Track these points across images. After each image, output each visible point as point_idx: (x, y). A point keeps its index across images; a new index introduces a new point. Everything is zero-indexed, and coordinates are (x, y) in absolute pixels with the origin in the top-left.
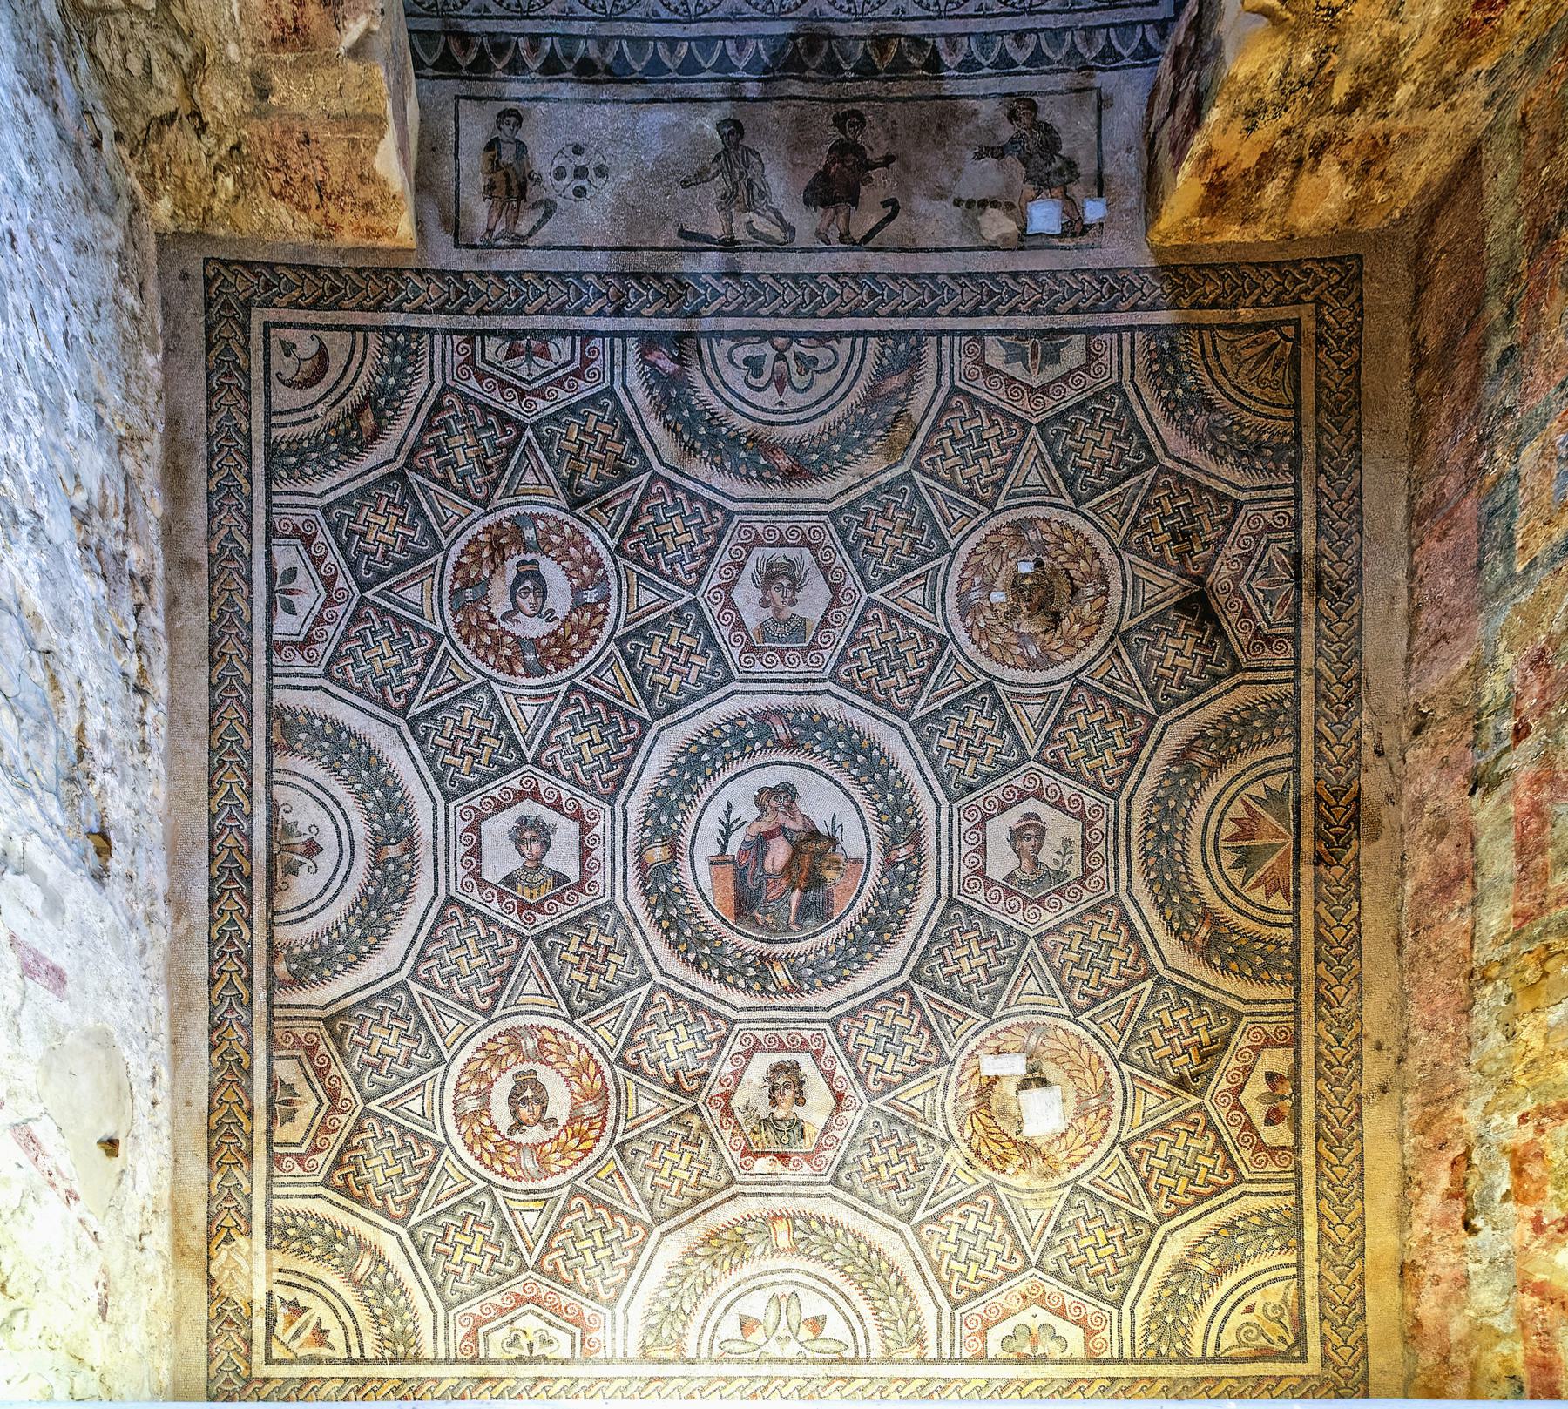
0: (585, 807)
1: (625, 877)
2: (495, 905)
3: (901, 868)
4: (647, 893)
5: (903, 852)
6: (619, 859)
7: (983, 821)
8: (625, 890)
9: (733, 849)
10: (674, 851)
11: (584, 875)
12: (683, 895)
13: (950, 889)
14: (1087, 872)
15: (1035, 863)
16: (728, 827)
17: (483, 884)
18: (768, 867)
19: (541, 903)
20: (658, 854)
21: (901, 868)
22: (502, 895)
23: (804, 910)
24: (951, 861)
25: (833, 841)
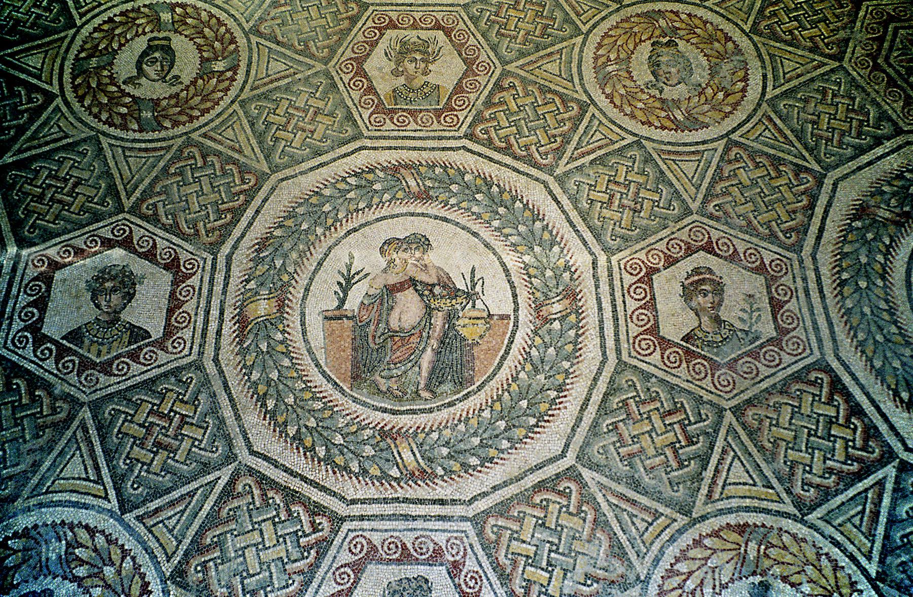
0: (183, 256)
1: (219, 333)
2: (50, 364)
3: (556, 325)
4: (243, 352)
5: (557, 307)
6: (215, 313)
7: (648, 274)
8: (217, 349)
9: (354, 302)
10: (281, 306)
11: (169, 332)
12: (287, 354)
13: (618, 351)
14: (782, 332)
15: (717, 320)
16: (348, 280)
17: (40, 339)
18: (394, 324)
19: (110, 363)
20: (262, 308)
21: (556, 325)
22: (62, 352)
23: (436, 377)
24: (616, 319)
25: (470, 296)
